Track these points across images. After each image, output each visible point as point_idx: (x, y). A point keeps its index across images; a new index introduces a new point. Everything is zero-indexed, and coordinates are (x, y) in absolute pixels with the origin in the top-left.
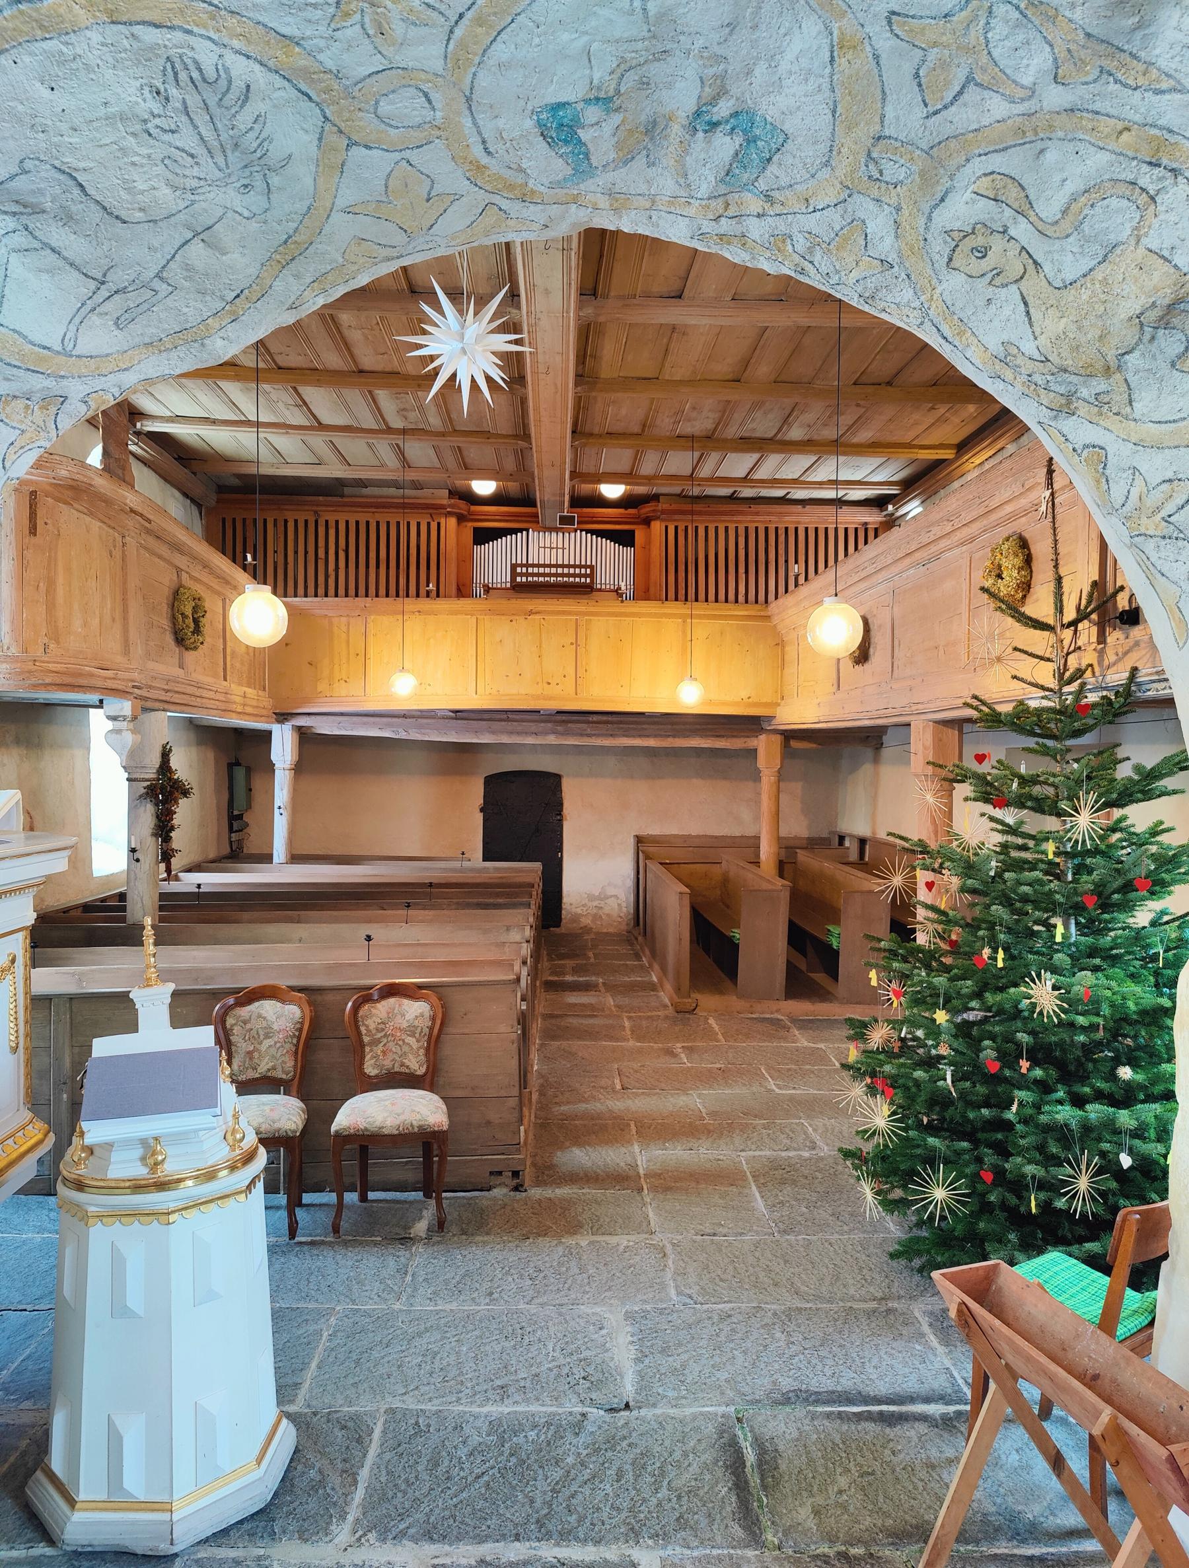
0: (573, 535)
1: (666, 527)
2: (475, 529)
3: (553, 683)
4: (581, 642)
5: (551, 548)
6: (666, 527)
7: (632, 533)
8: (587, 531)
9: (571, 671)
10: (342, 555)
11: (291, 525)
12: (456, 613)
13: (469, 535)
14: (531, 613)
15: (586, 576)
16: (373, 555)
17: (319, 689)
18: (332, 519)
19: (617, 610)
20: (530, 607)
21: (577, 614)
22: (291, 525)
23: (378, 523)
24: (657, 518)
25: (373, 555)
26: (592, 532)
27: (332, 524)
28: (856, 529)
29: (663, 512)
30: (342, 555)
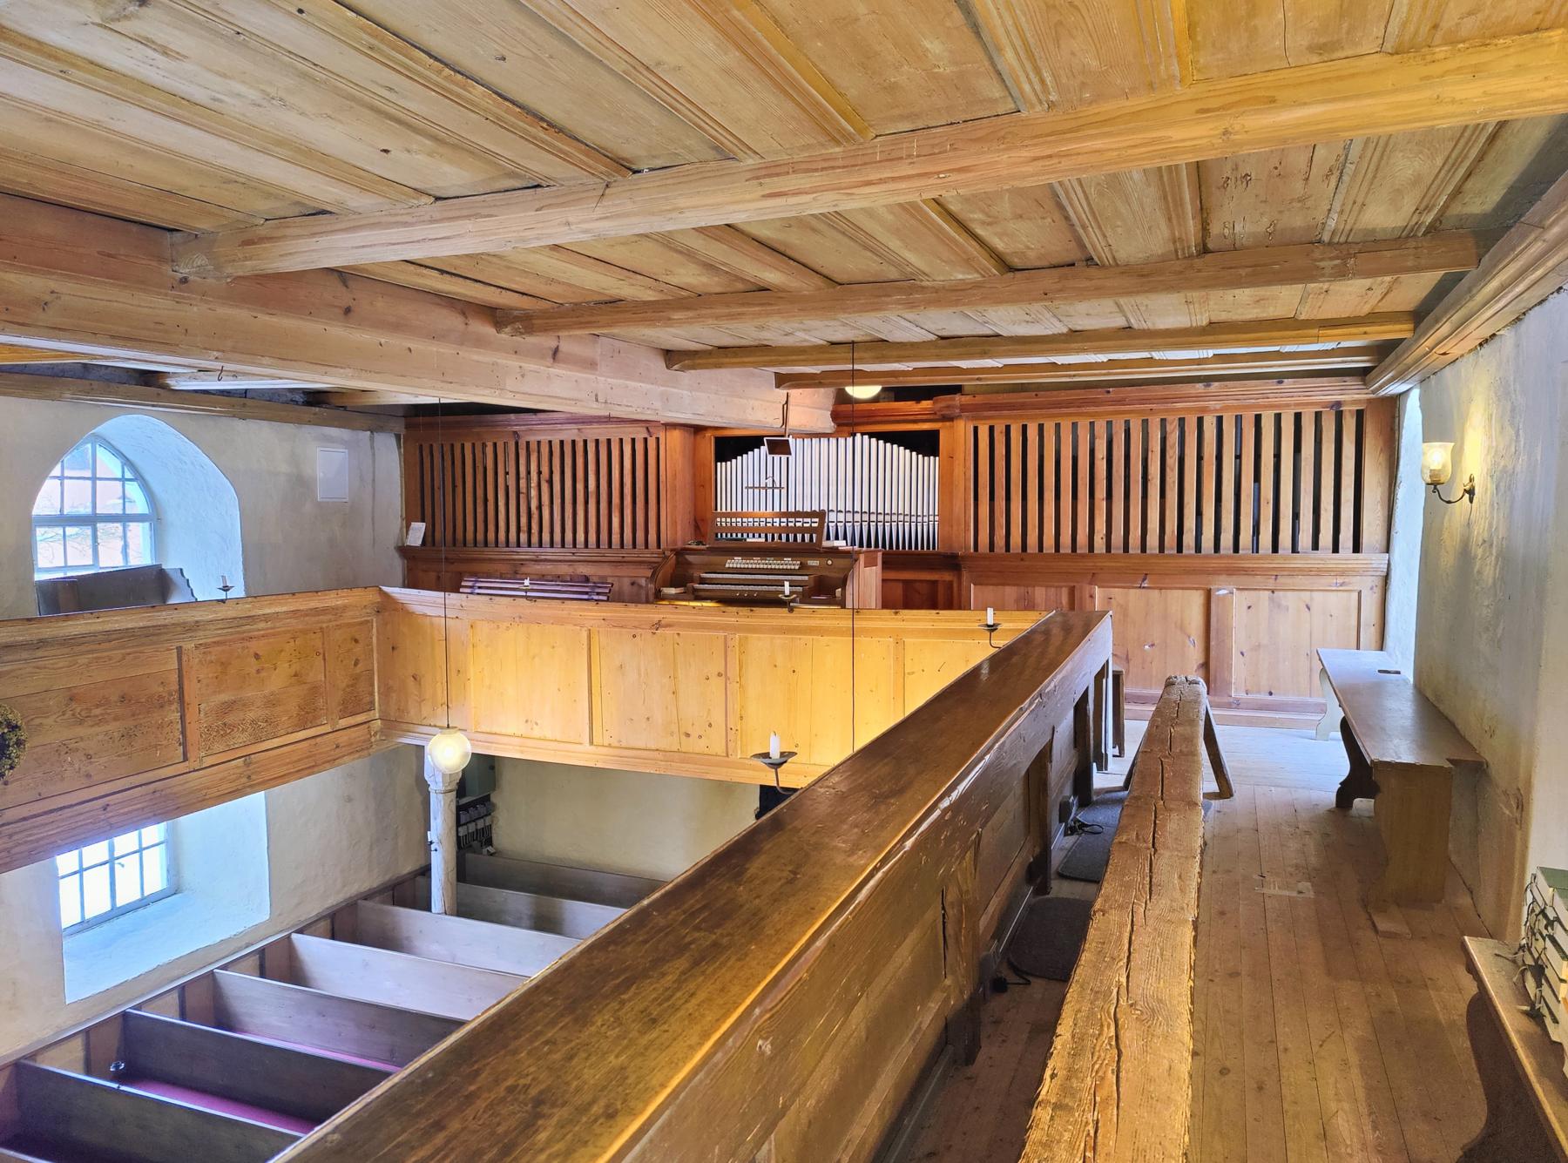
0: (850, 440)
1: (976, 429)
2: (718, 440)
3: (694, 735)
4: (733, 672)
5: (766, 488)
6: (976, 429)
7: (934, 435)
8: (871, 435)
9: (718, 717)
10: (545, 487)
11: (490, 450)
12: (560, 621)
13: (709, 449)
14: (658, 625)
15: (811, 530)
16: (580, 486)
17: (424, 714)
18: (533, 439)
19: (785, 622)
20: (656, 617)
21: (724, 628)
22: (490, 450)
23: (585, 442)
24: (959, 417)
25: (580, 486)
26: (879, 436)
27: (533, 447)
28: (1318, 415)
29: (964, 408)
30: (545, 487)
